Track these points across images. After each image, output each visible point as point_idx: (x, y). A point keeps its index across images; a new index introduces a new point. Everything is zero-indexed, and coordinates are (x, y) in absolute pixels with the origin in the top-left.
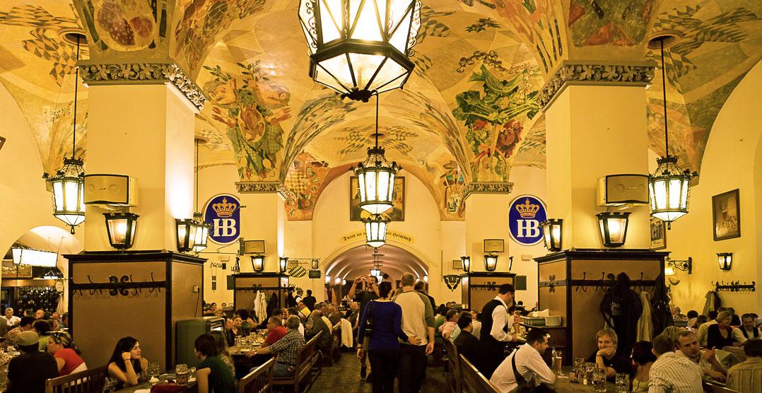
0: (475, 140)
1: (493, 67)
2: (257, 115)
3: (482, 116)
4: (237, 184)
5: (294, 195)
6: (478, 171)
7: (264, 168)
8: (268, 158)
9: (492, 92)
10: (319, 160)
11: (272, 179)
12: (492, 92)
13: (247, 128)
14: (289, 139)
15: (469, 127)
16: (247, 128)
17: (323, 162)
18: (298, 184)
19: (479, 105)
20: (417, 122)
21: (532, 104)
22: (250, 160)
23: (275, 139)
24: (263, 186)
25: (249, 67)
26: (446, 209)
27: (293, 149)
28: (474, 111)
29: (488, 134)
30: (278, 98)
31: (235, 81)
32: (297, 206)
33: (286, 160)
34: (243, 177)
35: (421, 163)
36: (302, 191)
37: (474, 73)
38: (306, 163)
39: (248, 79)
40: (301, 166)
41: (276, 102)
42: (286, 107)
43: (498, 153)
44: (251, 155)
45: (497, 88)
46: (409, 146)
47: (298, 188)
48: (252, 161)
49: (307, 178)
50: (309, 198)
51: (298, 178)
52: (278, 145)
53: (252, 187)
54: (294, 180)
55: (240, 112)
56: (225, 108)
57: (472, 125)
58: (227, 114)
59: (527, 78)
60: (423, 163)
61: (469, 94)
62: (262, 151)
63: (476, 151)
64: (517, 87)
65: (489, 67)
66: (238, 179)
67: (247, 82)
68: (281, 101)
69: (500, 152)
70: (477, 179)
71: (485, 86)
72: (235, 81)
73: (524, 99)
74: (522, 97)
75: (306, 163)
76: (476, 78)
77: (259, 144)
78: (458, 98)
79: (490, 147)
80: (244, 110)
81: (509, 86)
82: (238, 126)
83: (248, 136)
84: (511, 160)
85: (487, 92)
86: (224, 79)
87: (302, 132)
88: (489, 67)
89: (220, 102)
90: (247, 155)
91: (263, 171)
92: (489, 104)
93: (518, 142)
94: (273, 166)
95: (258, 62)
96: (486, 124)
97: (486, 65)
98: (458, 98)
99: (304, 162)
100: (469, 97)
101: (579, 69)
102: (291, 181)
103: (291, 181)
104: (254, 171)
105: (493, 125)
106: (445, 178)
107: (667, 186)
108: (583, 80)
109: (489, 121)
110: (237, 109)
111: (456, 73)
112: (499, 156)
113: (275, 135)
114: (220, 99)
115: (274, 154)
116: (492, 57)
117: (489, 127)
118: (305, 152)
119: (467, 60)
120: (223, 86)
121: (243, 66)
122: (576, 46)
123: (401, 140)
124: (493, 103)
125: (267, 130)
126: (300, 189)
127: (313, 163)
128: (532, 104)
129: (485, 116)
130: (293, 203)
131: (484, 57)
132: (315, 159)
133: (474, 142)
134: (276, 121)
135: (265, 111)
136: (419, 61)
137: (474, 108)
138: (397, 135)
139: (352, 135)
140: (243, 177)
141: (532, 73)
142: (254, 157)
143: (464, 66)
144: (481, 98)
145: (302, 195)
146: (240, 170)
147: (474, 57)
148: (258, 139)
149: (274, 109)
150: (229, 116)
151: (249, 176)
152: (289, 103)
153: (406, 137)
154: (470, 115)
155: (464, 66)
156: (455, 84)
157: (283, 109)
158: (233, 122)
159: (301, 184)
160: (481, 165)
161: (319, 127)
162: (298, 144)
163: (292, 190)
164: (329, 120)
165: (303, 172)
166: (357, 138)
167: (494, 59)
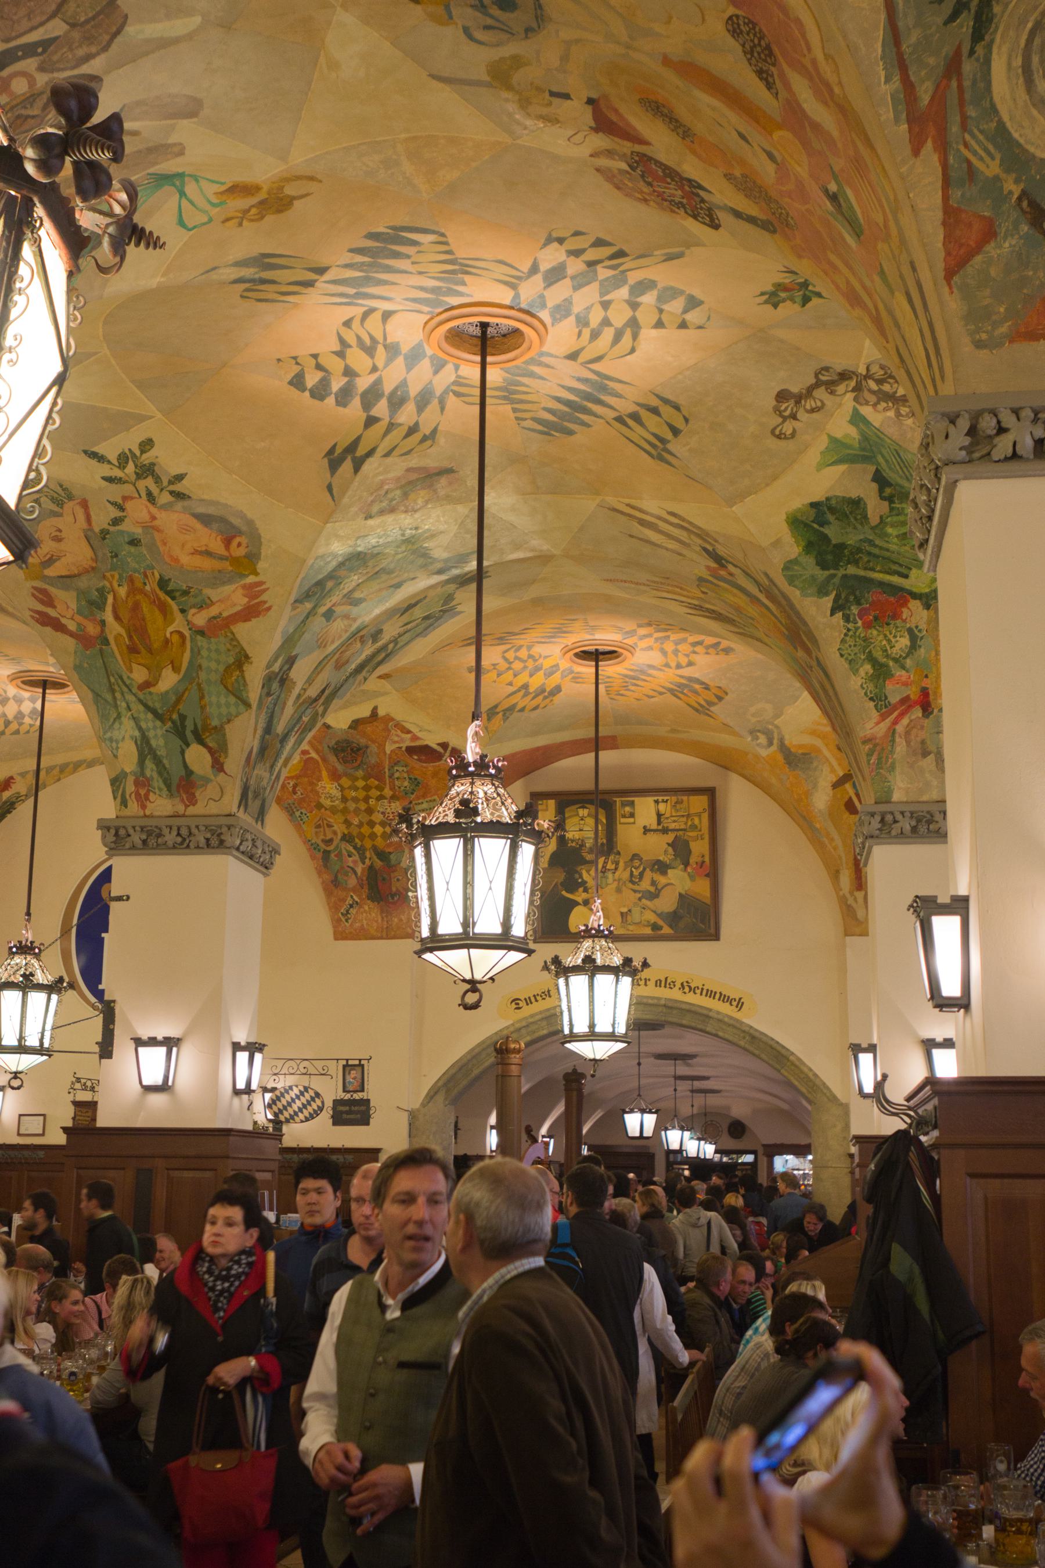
0: (871, 659)
1: (891, 414)
2: (163, 609)
3: (887, 578)
4: (104, 826)
5: (357, 857)
6: (892, 768)
7: (189, 773)
8: (201, 742)
10: (432, 740)
11: (214, 809)
13: (133, 650)
14: (269, 679)
15: (847, 618)
16: (133, 650)
17: (444, 745)
18: (365, 818)
19: (871, 543)
20: (700, 608)
22: (145, 749)
23: (223, 682)
24: (184, 832)
25: (123, 460)
27: (289, 710)
28: (856, 563)
30: (222, 551)
31: (84, 504)
32: (366, 889)
33: (263, 749)
34: (124, 803)
35: (763, 739)
37: (833, 440)
38: (389, 748)
39: (125, 498)
40: (373, 760)
41: (218, 565)
42: (251, 579)
44: (151, 734)
46: (711, 684)
47: (366, 830)
48: (152, 752)
49: (394, 798)
51: (366, 799)
52: (232, 700)
53: (149, 833)
54: (351, 806)
55: (110, 599)
56: (66, 588)
57: (855, 610)
58: (73, 605)
60: (770, 743)
61: (832, 510)
62: (183, 718)
63: (878, 699)
65: (878, 416)
66: (109, 810)
67: (122, 509)
68: (235, 561)
70: (889, 792)
71: (879, 479)
72: (84, 504)
75: (389, 748)
76: (840, 453)
77: (174, 698)
78: (795, 522)
79: (927, 683)
80: (122, 592)
82: (106, 642)
83: (139, 675)
85: (890, 499)
86: (53, 499)
87: (316, 656)
88: (878, 416)
89: (51, 572)
90: (137, 733)
91: (186, 785)
94: (218, 766)
95: (147, 445)
96: (905, 604)
97: (866, 411)
98: (795, 522)
99: (382, 747)
100: (831, 518)
101: (988, 424)
102: (345, 811)
103: (345, 811)
104: (158, 783)
105: (927, 607)
106: (848, 786)
107: (468, 855)
108: (1007, 459)
109: (915, 596)
110: (102, 592)
111: (772, 443)
113: (222, 668)
114: (50, 562)
115: (219, 730)
116: (879, 382)
118: (381, 712)
119: (799, 399)
120: (54, 521)
121: (101, 459)
122: (979, 345)
123: (679, 666)
125: (196, 653)
126: (373, 836)
127: (410, 750)
129: (895, 580)
130: (352, 882)
131: (853, 383)
132: (415, 738)
133: (868, 667)
134: (220, 626)
135: (186, 593)
136: (644, 414)
137: (854, 556)
138: (664, 653)
139: (511, 655)
140: (124, 803)
142: (159, 736)
143: (794, 417)
144: (874, 520)
145: (382, 855)
146: (116, 782)
147: (818, 384)
148: (168, 680)
149: (214, 586)
150: (79, 612)
151: (143, 801)
152: (261, 566)
153: (694, 658)
154: (845, 576)
155: (794, 417)
156: (775, 478)
157: (244, 587)
158: (92, 630)
159: (377, 817)
160: (901, 748)
161: (385, 638)
162: (313, 692)
163: (347, 838)
164: (418, 613)
165: (380, 777)
166: (530, 664)
167: (886, 387)
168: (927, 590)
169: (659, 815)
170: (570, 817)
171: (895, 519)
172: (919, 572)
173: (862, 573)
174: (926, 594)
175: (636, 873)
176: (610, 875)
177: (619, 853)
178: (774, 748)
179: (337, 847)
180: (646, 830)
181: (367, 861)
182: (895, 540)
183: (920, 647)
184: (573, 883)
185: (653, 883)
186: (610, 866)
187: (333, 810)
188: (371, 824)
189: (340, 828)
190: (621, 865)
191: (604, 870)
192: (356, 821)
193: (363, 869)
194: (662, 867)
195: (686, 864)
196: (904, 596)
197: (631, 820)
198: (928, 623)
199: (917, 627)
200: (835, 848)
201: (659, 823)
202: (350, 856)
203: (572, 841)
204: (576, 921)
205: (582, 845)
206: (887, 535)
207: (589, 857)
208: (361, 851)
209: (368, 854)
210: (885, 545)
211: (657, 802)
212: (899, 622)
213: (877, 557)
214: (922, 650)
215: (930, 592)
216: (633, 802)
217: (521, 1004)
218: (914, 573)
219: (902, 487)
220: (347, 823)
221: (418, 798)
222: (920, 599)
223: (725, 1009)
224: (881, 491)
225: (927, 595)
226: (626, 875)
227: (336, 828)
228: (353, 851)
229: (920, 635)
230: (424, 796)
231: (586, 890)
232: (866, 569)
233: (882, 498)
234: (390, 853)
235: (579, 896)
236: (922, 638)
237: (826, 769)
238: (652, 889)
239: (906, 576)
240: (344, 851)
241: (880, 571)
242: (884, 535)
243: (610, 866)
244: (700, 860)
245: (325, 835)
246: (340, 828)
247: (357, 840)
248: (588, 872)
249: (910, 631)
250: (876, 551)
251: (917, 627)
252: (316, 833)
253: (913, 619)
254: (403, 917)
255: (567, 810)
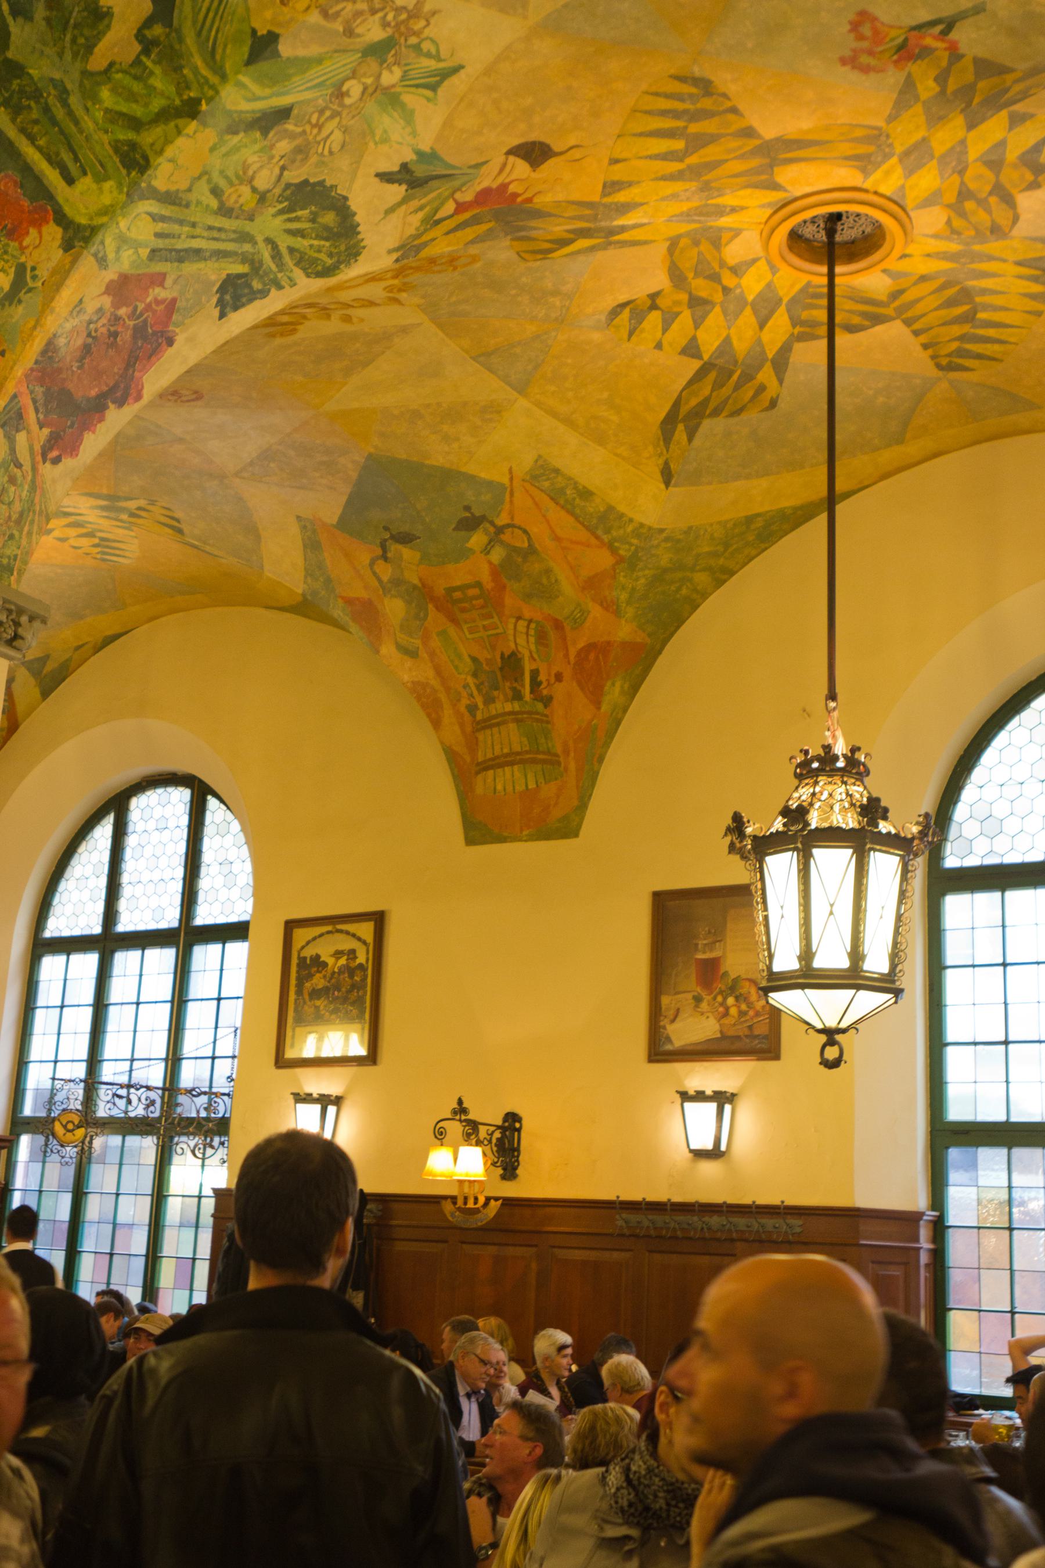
9: (173, 59)
12: (173, 59)
19: (63, 94)
21: (269, 241)
29: (19, 283)
43: (20, 416)
45: (211, 56)
59: (354, 88)
64: (284, 114)
69: (31, 417)
73: (262, 198)
74: (264, 180)
81: (259, 80)
84: (60, 479)
85: (148, 46)
92: (115, 117)
93: (121, 403)
105: (67, 246)
109: (61, 219)
112: (21, 438)
117: (45, 245)
124: (135, 124)
128: (269, 241)
129: (52, 176)
141: (390, 77)
144: (98, 61)
168: (83, 221)
171: (127, 80)
172: (94, 186)
173: (12, 133)
174: (79, 225)
182: (99, 115)
183: (20, 301)
196: (46, 207)
198: (54, 272)
199: (33, 269)
206: (95, 98)
210: (80, 112)
212: (14, 245)
213: (54, 122)
214: (20, 309)
215: (85, 227)
218: (86, 183)
219: (181, 40)
222: (66, 229)
224: (149, 23)
225: (79, 228)
229: (31, 284)
232: (23, 131)
233: (140, 36)
236: (30, 290)
239: (70, 181)
241: (39, 149)
242: (91, 96)
249: (21, 269)
250: (59, 113)
251: (33, 269)
253: (35, 253)
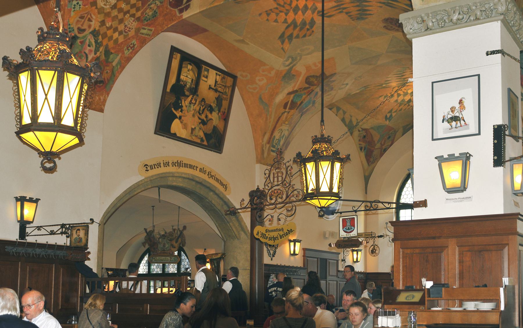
5: (93, 48)
26: (268, 146)
36: (111, 44)
50: (114, 64)
103: (108, 15)
163: (95, 33)
169: (216, 82)
170: (184, 67)
175: (201, 109)
176: (192, 105)
177: (198, 96)
178: (287, 68)
179: (85, 37)
180: (210, 88)
181: (98, 54)
184: (178, 106)
185: (206, 117)
186: (193, 101)
187: (101, 11)
188: (116, 30)
189: (95, 24)
190: (197, 102)
191: (191, 103)
192: (108, 25)
193: (93, 58)
194: (211, 110)
195: (219, 111)
197: (206, 79)
200: (270, 122)
201: (215, 86)
202: (89, 46)
203: (183, 81)
204: (176, 126)
205: (185, 85)
207: (187, 93)
208: (98, 45)
209: (101, 49)
211: (217, 74)
216: (209, 70)
217: (149, 168)
220: (103, 23)
221: (146, 25)
223: (221, 188)
226: (198, 109)
227: (92, 23)
228: (94, 43)
230: (149, 25)
231: (181, 111)
234: (112, 53)
235: (178, 114)
237: (293, 85)
238: (205, 119)
240: (87, 42)
243: (193, 101)
244: (224, 111)
245: (82, 25)
246: (95, 24)
247: (100, 37)
248: (185, 101)
252: (78, 21)
254: (102, 98)
255: (184, 62)
